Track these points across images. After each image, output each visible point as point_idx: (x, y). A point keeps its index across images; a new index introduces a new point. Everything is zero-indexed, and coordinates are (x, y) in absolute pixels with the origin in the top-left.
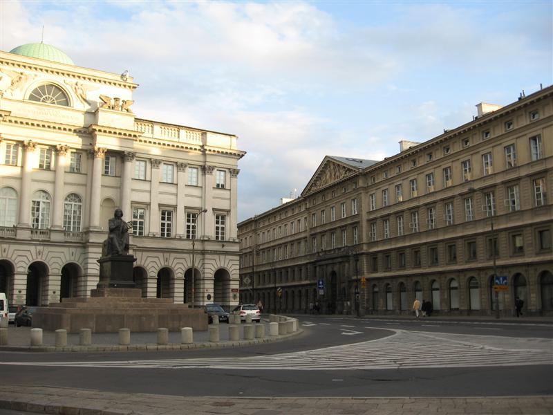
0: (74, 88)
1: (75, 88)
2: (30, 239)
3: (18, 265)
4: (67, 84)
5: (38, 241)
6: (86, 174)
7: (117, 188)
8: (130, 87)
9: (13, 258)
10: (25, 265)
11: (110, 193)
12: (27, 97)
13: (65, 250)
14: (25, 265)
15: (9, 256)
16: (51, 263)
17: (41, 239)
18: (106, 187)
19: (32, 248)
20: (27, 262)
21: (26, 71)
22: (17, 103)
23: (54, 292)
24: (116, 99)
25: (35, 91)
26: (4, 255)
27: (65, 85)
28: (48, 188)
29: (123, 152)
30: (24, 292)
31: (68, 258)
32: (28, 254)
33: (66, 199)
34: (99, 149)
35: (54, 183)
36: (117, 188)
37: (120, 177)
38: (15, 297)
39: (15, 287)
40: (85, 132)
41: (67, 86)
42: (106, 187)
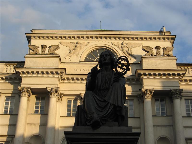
0: (120, 47)
1: (122, 47)
4: (114, 45)
6: (139, 118)
7: (169, 126)
8: (168, 39)
11: (163, 132)
12: (83, 60)
18: (159, 126)
21: (81, 41)
22: (75, 66)
24: (157, 48)
25: (89, 55)
27: (113, 46)
29: (170, 91)
34: (146, 90)
36: (169, 126)
37: (172, 116)
40: (133, 80)
41: (115, 47)
42: (159, 126)
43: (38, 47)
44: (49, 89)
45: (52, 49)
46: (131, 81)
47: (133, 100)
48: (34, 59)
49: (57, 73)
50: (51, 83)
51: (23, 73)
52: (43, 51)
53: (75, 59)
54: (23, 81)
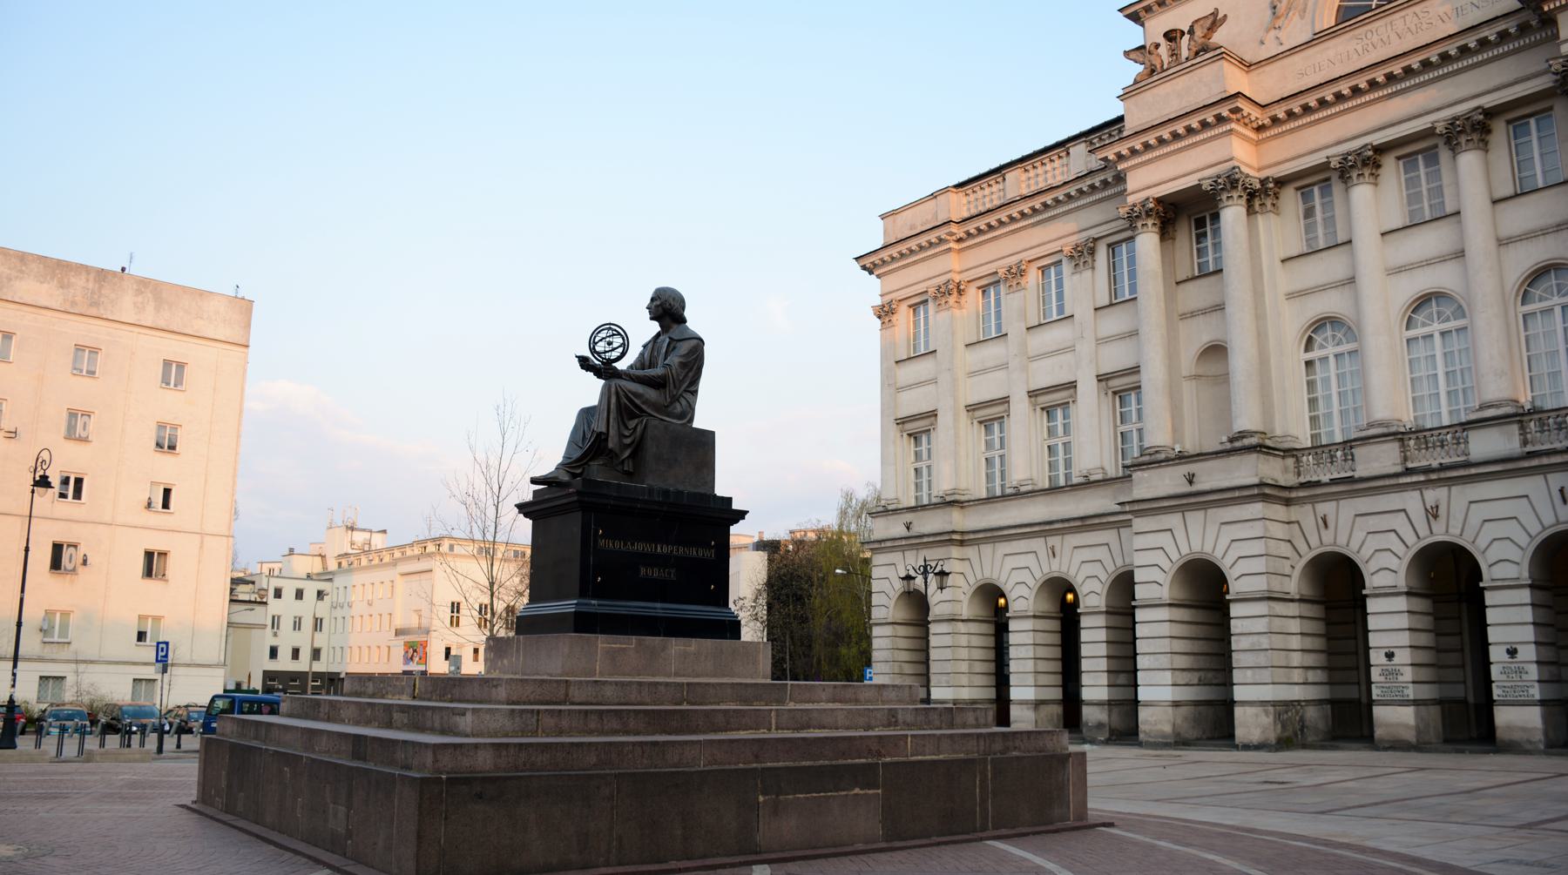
2: (1399, 469)
3: (1373, 566)
5: (1427, 470)
9: (1354, 545)
10: (1393, 563)
13: (1532, 485)
14: (1393, 563)
15: (1342, 540)
16: (1482, 542)
17: (1435, 464)
19: (1412, 501)
20: (1398, 547)
22: (1297, 58)
23: (1512, 652)
26: (1328, 536)
28: (1441, 278)
30: (1528, 653)
31: (1548, 519)
32: (1398, 521)
33: (1525, 299)
35: (1460, 254)
38: (1375, 674)
39: (1374, 640)
43: (1157, 46)
44: (1206, 186)
45: (1199, 33)
46: (1517, 38)
47: (1551, 108)
48: (1148, 96)
49: (1220, 119)
50: (1213, 159)
51: (1120, 157)
52: (1174, 54)
53: (1296, 31)
54: (1132, 182)
